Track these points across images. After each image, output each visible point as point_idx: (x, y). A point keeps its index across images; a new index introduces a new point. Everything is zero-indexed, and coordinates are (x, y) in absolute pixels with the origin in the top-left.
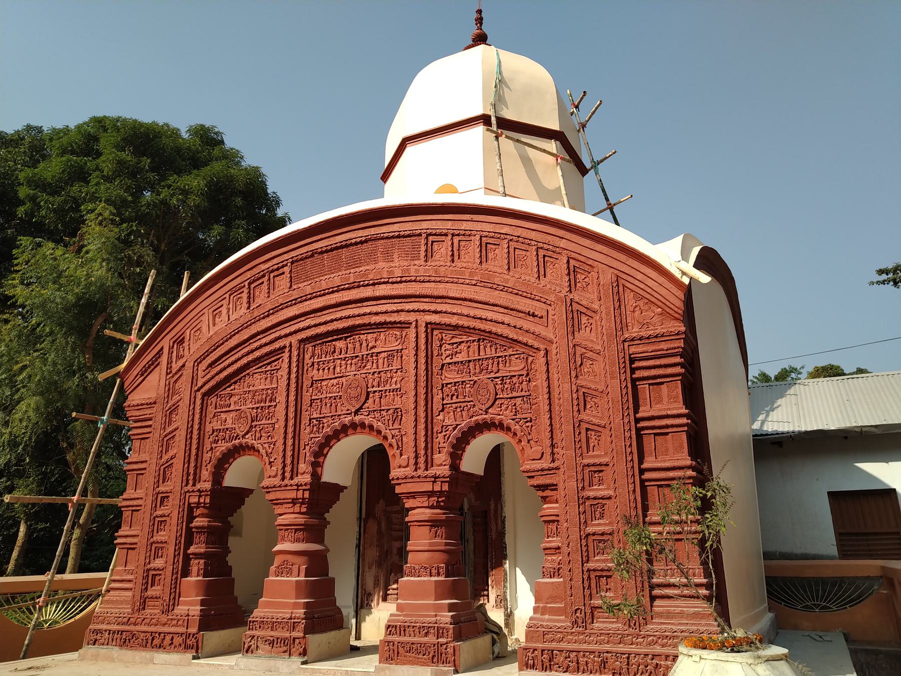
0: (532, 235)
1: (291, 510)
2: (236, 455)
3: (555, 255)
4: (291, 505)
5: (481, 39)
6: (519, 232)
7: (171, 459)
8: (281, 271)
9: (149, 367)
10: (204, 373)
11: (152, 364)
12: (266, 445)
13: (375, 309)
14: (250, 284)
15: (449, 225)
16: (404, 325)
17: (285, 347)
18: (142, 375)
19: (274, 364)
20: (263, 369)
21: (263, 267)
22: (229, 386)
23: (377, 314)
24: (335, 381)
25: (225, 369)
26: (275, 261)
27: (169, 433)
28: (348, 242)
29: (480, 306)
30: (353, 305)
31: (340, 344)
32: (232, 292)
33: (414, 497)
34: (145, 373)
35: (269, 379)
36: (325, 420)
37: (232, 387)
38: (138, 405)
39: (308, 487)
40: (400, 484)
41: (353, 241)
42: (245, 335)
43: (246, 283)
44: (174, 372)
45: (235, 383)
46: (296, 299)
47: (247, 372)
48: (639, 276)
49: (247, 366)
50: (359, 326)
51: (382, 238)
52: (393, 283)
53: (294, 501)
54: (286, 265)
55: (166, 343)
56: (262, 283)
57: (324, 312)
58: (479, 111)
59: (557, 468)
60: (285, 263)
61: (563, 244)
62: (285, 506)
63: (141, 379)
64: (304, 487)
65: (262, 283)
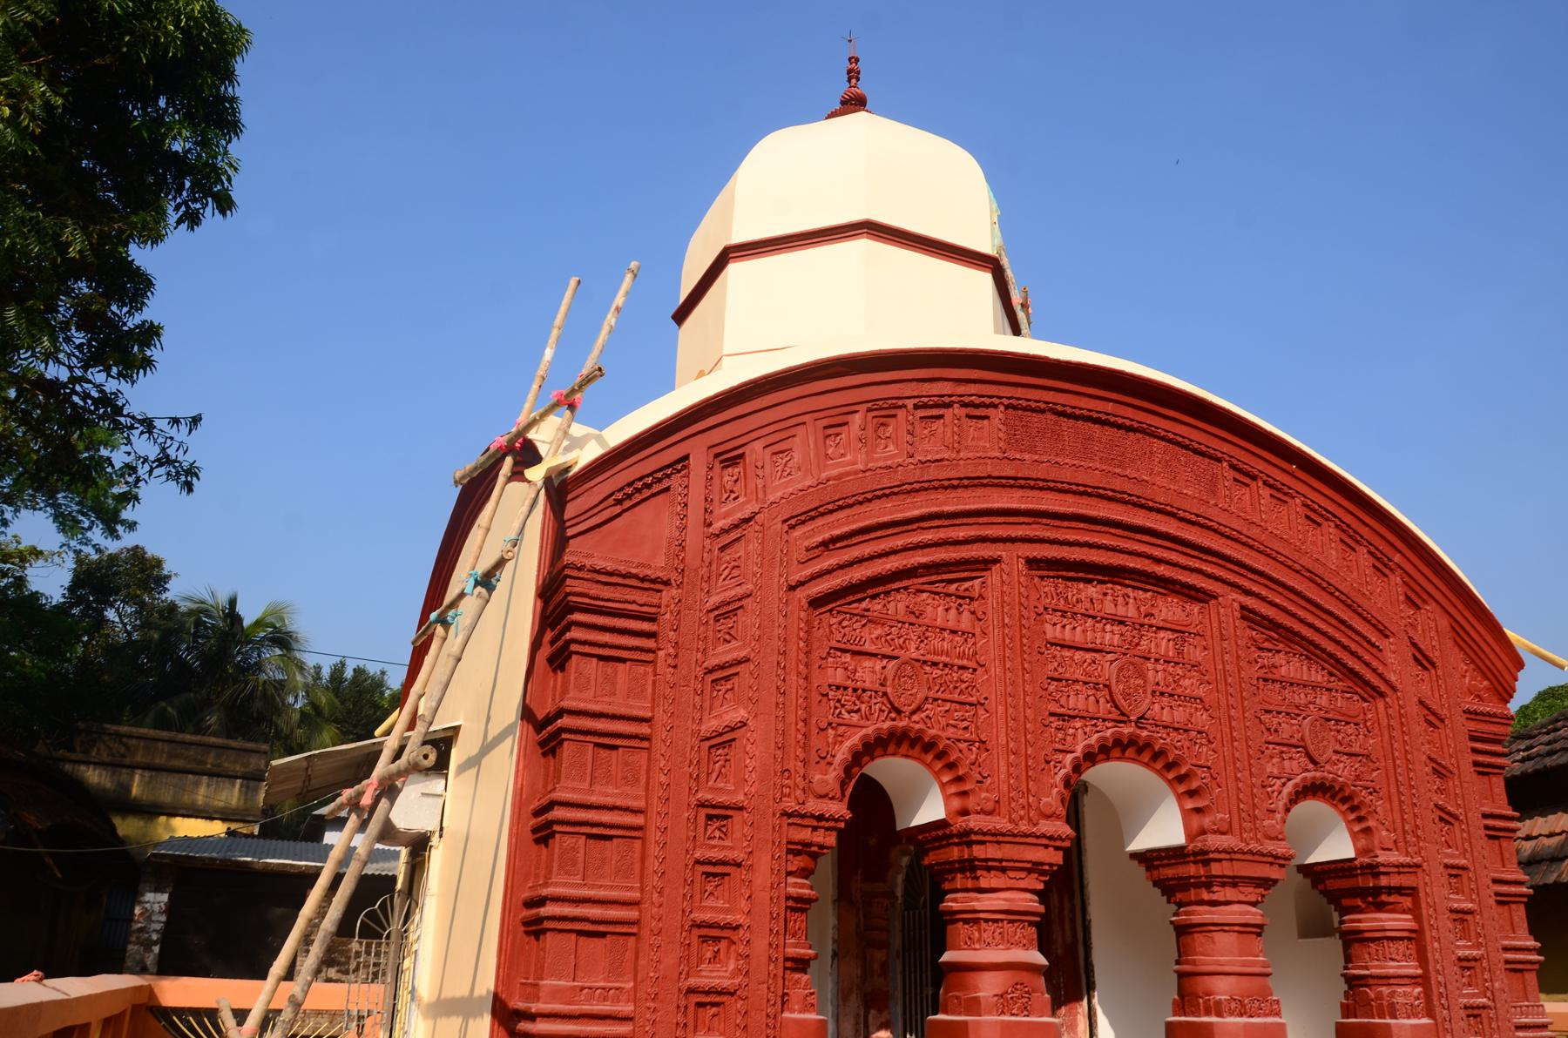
0: (1364, 531)
1: (1022, 884)
2: (879, 751)
3: (1387, 571)
4: (1023, 874)
5: (854, 103)
6: (1348, 519)
7: (733, 729)
8: (981, 412)
9: (638, 491)
10: (803, 556)
11: (648, 486)
12: (963, 746)
13: (1156, 552)
14: (916, 407)
15: (1261, 466)
16: (1202, 596)
17: (997, 561)
18: (618, 502)
19: (967, 585)
20: (939, 587)
21: (946, 388)
22: (860, 601)
23: (1159, 561)
24: (1088, 656)
25: (860, 561)
26: (973, 389)
27: (721, 667)
28: (1112, 419)
29: (1303, 603)
30: (1119, 532)
31: (1092, 591)
32: (874, 406)
33: (1235, 885)
34: (630, 498)
35: (953, 612)
36: (1078, 724)
37: (864, 605)
38: (611, 574)
39: (1067, 844)
40: (1220, 860)
41: (1120, 421)
42: (1260, 563)
43: (910, 403)
44: (718, 525)
45: (874, 597)
46: (1016, 479)
47: (905, 583)
48: (1476, 636)
49: (910, 573)
50: (1133, 571)
51: (1162, 439)
52: (1182, 519)
53: (1035, 868)
54: (996, 406)
55: (698, 451)
56: (942, 416)
57: (1066, 524)
58: (987, 249)
59: (1418, 866)
60: (996, 401)
61: (1397, 558)
62: (1012, 874)
63: (618, 509)
64: (1058, 843)
65: (942, 416)
